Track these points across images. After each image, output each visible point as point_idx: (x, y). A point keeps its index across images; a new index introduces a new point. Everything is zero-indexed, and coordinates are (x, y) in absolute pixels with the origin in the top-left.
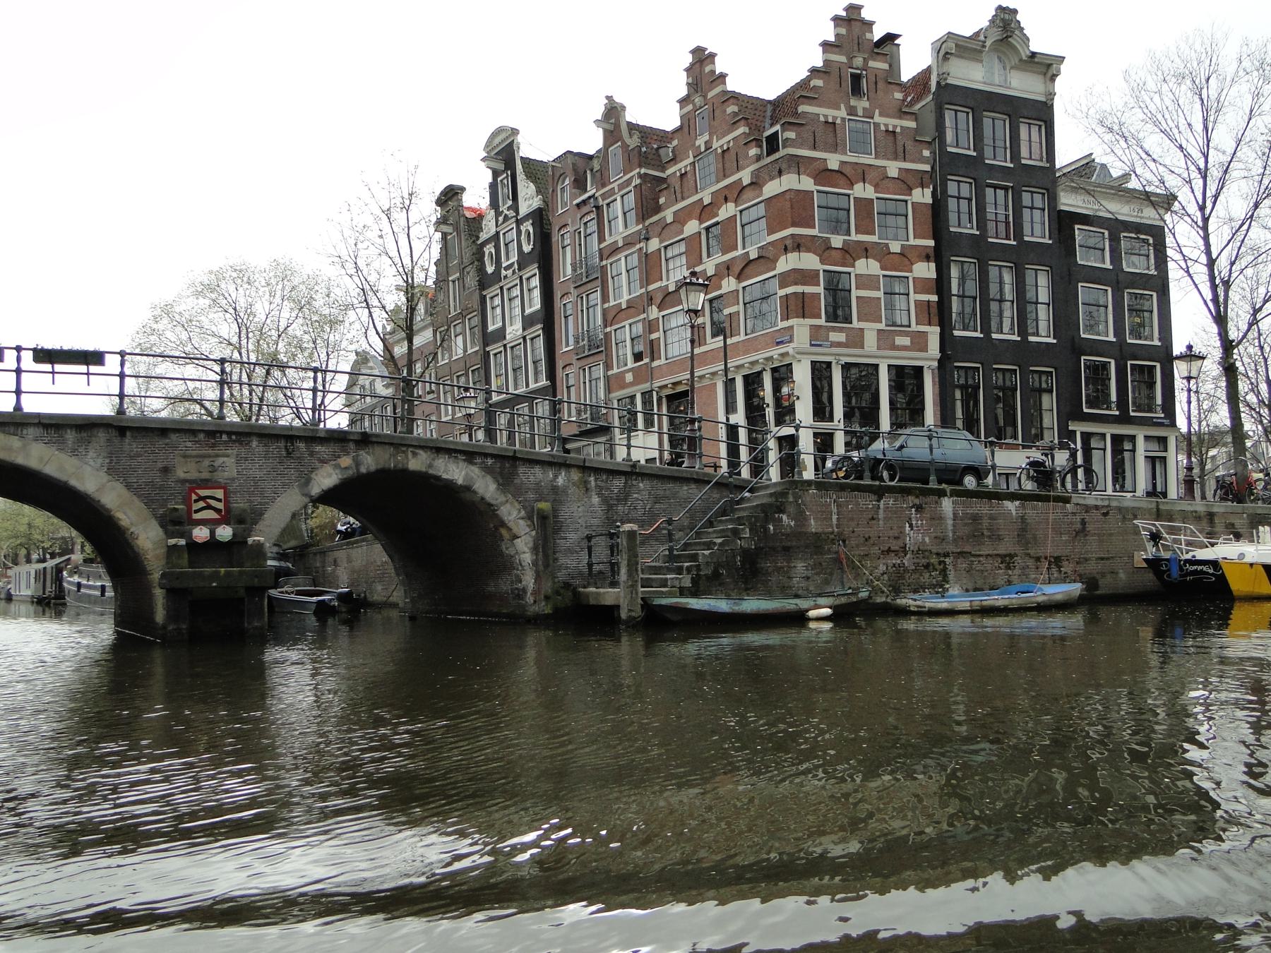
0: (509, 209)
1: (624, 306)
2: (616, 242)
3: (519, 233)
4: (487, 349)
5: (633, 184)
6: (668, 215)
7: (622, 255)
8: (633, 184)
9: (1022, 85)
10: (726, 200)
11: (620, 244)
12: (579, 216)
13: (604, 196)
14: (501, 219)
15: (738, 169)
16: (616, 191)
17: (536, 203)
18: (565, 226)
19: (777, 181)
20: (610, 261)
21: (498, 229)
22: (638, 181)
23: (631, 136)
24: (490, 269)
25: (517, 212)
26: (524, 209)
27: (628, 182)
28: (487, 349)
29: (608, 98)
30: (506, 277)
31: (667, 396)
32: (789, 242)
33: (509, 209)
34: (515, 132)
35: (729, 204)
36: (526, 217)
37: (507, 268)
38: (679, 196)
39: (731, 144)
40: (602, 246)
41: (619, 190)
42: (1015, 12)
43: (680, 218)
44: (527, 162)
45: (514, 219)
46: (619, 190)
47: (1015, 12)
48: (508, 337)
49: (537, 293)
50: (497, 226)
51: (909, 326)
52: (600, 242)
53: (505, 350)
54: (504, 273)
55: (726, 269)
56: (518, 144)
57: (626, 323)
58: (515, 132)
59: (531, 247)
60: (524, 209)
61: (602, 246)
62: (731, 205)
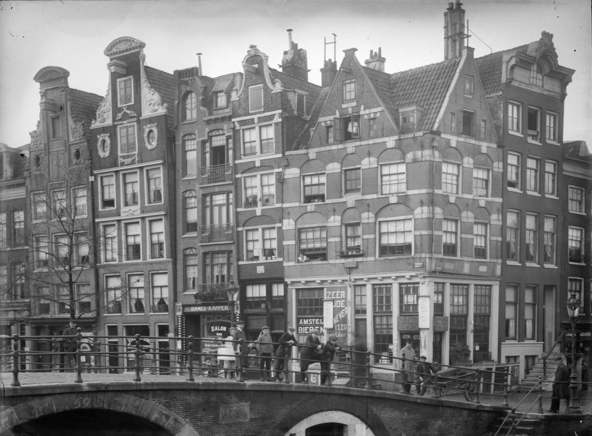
0: (129, 108)
1: (259, 213)
2: (254, 162)
3: (141, 130)
4: (97, 220)
5: (275, 121)
6: (312, 153)
7: (258, 174)
8: (275, 121)
11: (258, 164)
12: (207, 130)
13: (242, 123)
14: (120, 115)
15: (383, 136)
16: (256, 121)
17: (162, 111)
18: (190, 134)
20: (244, 175)
21: (116, 123)
22: (280, 120)
23: (273, 83)
24: (104, 154)
25: (140, 115)
26: (146, 113)
27: (271, 118)
28: (97, 220)
29: (252, 47)
30: (123, 164)
33: (129, 108)
34: (142, 46)
36: (150, 120)
37: (124, 157)
39: (378, 115)
40: (237, 162)
41: (259, 122)
42: (552, 36)
45: (135, 119)
46: (259, 122)
47: (552, 36)
48: (122, 214)
50: (114, 120)
52: (235, 158)
53: (119, 225)
54: (120, 160)
56: (144, 56)
57: (260, 227)
59: (154, 144)
60: (146, 113)
61: (237, 162)
62: (373, 159)
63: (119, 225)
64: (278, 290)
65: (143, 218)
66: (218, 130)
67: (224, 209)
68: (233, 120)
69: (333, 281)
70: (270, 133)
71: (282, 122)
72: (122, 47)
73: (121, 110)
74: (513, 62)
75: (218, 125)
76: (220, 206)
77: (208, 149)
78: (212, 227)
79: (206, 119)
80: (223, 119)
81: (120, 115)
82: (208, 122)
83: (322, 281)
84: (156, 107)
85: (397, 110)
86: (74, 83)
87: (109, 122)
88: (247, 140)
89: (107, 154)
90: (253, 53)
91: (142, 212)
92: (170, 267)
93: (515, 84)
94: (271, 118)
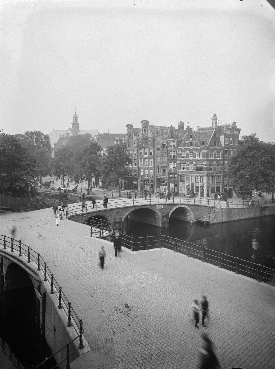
9: (236, 133)
14: (144, 136)
17: (152, 136)
27: (175, 140)
34: (149, 122)
36: (150, 138)
55: (193, 160)
57: (173, 162)
63: (143, 159)
64: (176, 176)
65: (148, 158)
67: (165, 157)
72: (144, 122)
73: (144, 135)
75: (164, 140)
76: (165, 157)
77: (162, 145)
80: (165, 139)
81: (144, 136)
82: (162, 139)
85: (200, 141)
86: (133, 127)
87: (141, 137)
89: (141, 143)
91: (148, 157)
92: (154, 168)
94: (175, 140)
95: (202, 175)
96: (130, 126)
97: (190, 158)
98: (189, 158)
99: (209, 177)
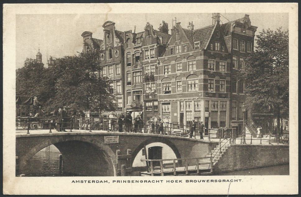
2: (148, 61)
5: (155, 47)
7: (150, 65)
8: (155, 47)
9: (248, 33)
10: (184, 58)
16: (149, 48)
19: (200, 57)
22: (156, 47)
23: (154, 35)
27: (153, 46)
29: (148, 23)
31: (162, 103)
32: (202, 72)
34: (114, 24)
35: (185, 59)
36: (116, 48)
38: (170, 53)
43: (170, 60)
44: (116, 32)
49: (120, 69)
51: (224, 92)
54: (107, 61)
58: (114, 24)
62: (186, 60)
64: (156, 103)
66: (137, 51)
67: (140, 77)
68: (142, 47)
69: (173, 100)
70: (153, 52)
71: (157, 48)
73: (108, 45)
74: (234, 25)
77: (135, 57)
78: (136, 83)
79: (134, 47)
80: (139, 47)
82: (134, 48)
83: (170, 100)
84: (118, 44)
86: (94, 36)
88: (146, 55)
90: (148, 25)
93: (235, 32)
94: (153, 46)
95: (197, 98)
96: (88, 34)
97: (176, 72)
98: (175, 72)
99: (208, 101)
